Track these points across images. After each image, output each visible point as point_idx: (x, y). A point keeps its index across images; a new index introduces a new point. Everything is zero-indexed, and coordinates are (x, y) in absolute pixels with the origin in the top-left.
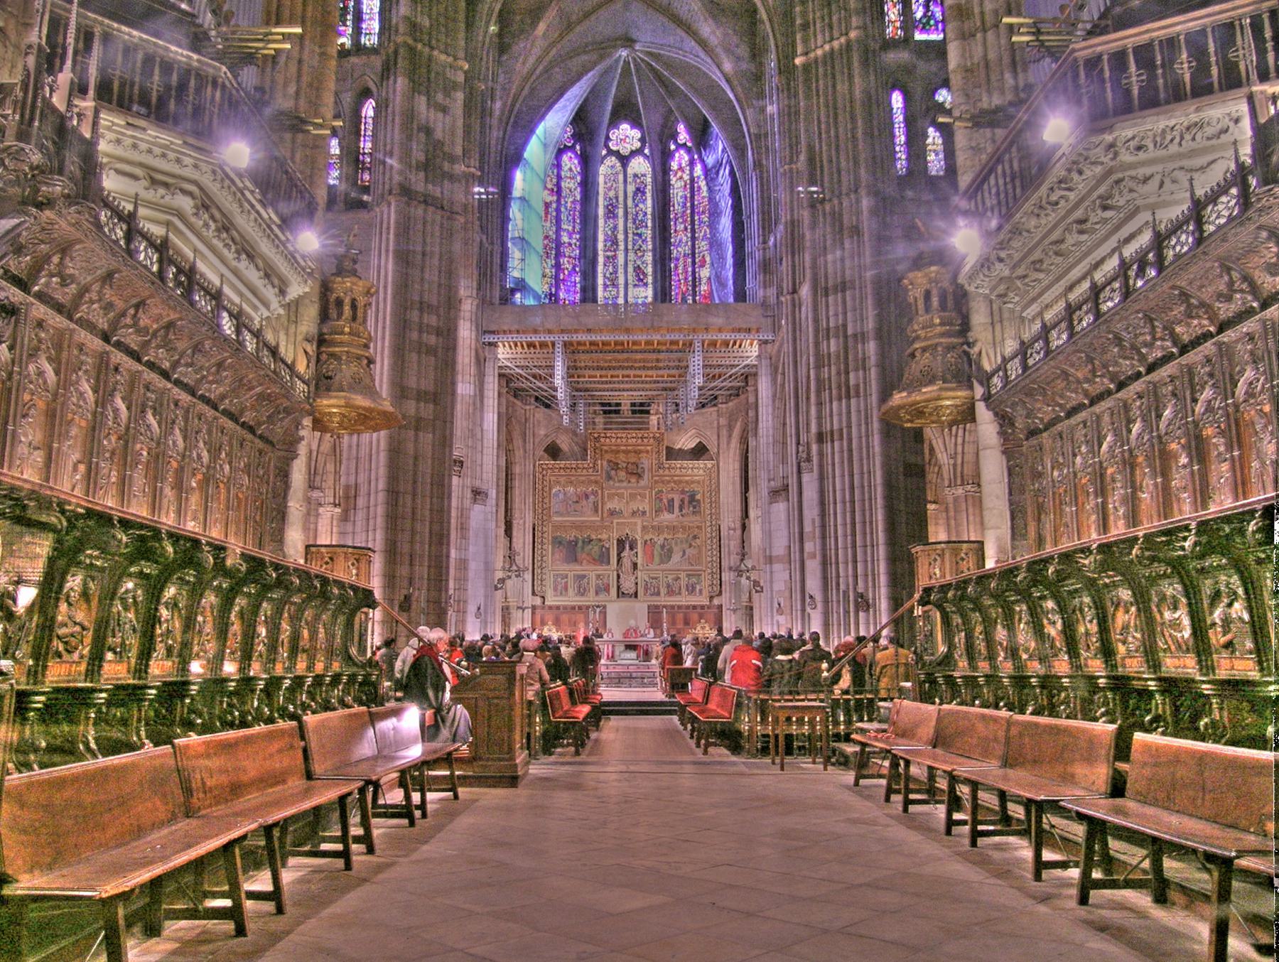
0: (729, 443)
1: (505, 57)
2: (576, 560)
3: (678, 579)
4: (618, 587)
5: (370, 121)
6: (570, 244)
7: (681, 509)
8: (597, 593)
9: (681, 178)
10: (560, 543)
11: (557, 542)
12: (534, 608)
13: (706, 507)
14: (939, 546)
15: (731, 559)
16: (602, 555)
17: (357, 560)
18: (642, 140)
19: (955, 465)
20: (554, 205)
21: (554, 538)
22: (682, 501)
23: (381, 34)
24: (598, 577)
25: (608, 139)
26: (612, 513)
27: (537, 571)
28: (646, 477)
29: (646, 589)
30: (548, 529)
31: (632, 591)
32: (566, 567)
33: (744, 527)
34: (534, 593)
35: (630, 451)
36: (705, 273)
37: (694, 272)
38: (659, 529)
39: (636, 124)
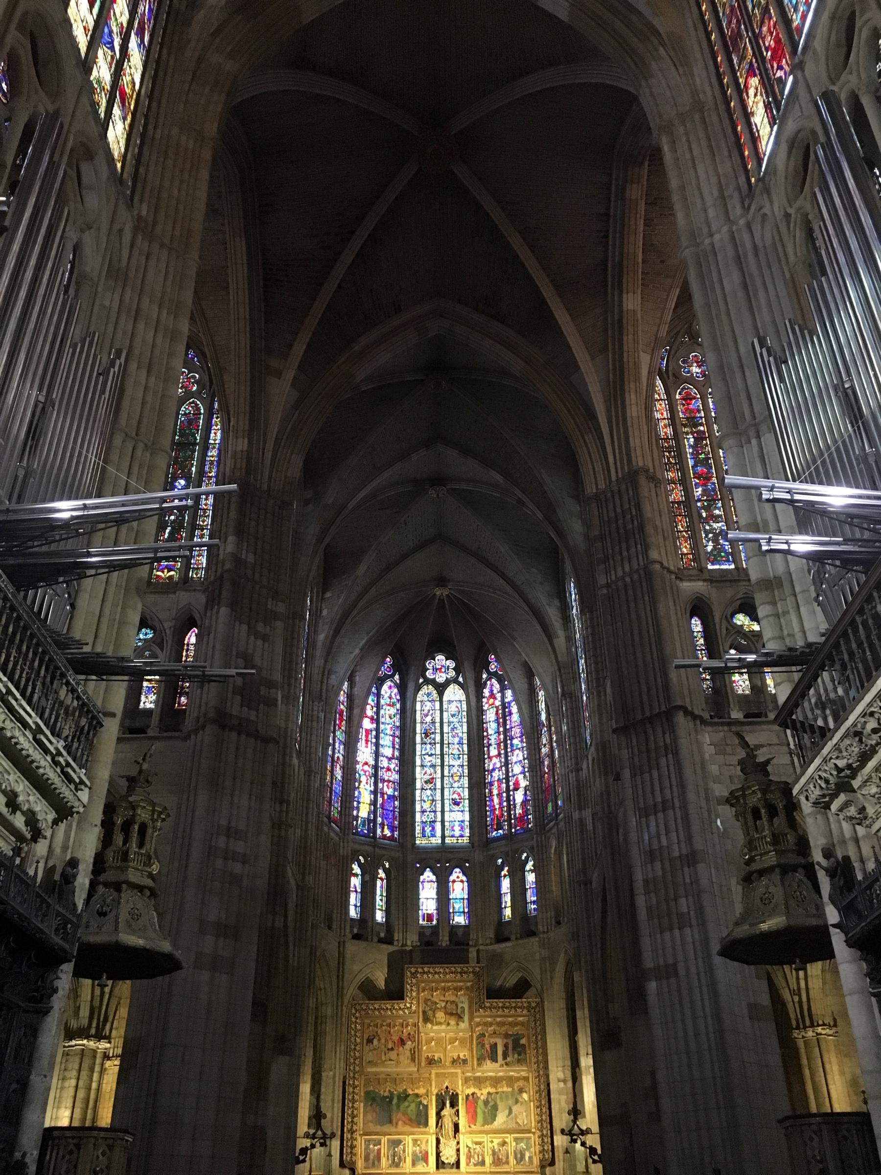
0: (552, 978)
1: (328, 595)
2: (391, 1122)
3: (504, 1143)
5: (192, 648)
6: (388, 769)
8: (414, 1164)
9: (493, 704)
10: (373, 1099)
11: (371, 1098)
13: (531, 1053)
14: (812, 1120)
15: (561, 1120)
17: (111, 1147)
18: (456, 669)
19: (800, 1002)
20: (374, 733)
21: (367, 1093)
22: (506, 1046)
23: (207, 569)
24: (415, 1141)
26: (431, 1062)
28: (466, 1018)
29: (469, 1157)
31: (453, 1160)
32: (378, 1129)
37: (508, 796)
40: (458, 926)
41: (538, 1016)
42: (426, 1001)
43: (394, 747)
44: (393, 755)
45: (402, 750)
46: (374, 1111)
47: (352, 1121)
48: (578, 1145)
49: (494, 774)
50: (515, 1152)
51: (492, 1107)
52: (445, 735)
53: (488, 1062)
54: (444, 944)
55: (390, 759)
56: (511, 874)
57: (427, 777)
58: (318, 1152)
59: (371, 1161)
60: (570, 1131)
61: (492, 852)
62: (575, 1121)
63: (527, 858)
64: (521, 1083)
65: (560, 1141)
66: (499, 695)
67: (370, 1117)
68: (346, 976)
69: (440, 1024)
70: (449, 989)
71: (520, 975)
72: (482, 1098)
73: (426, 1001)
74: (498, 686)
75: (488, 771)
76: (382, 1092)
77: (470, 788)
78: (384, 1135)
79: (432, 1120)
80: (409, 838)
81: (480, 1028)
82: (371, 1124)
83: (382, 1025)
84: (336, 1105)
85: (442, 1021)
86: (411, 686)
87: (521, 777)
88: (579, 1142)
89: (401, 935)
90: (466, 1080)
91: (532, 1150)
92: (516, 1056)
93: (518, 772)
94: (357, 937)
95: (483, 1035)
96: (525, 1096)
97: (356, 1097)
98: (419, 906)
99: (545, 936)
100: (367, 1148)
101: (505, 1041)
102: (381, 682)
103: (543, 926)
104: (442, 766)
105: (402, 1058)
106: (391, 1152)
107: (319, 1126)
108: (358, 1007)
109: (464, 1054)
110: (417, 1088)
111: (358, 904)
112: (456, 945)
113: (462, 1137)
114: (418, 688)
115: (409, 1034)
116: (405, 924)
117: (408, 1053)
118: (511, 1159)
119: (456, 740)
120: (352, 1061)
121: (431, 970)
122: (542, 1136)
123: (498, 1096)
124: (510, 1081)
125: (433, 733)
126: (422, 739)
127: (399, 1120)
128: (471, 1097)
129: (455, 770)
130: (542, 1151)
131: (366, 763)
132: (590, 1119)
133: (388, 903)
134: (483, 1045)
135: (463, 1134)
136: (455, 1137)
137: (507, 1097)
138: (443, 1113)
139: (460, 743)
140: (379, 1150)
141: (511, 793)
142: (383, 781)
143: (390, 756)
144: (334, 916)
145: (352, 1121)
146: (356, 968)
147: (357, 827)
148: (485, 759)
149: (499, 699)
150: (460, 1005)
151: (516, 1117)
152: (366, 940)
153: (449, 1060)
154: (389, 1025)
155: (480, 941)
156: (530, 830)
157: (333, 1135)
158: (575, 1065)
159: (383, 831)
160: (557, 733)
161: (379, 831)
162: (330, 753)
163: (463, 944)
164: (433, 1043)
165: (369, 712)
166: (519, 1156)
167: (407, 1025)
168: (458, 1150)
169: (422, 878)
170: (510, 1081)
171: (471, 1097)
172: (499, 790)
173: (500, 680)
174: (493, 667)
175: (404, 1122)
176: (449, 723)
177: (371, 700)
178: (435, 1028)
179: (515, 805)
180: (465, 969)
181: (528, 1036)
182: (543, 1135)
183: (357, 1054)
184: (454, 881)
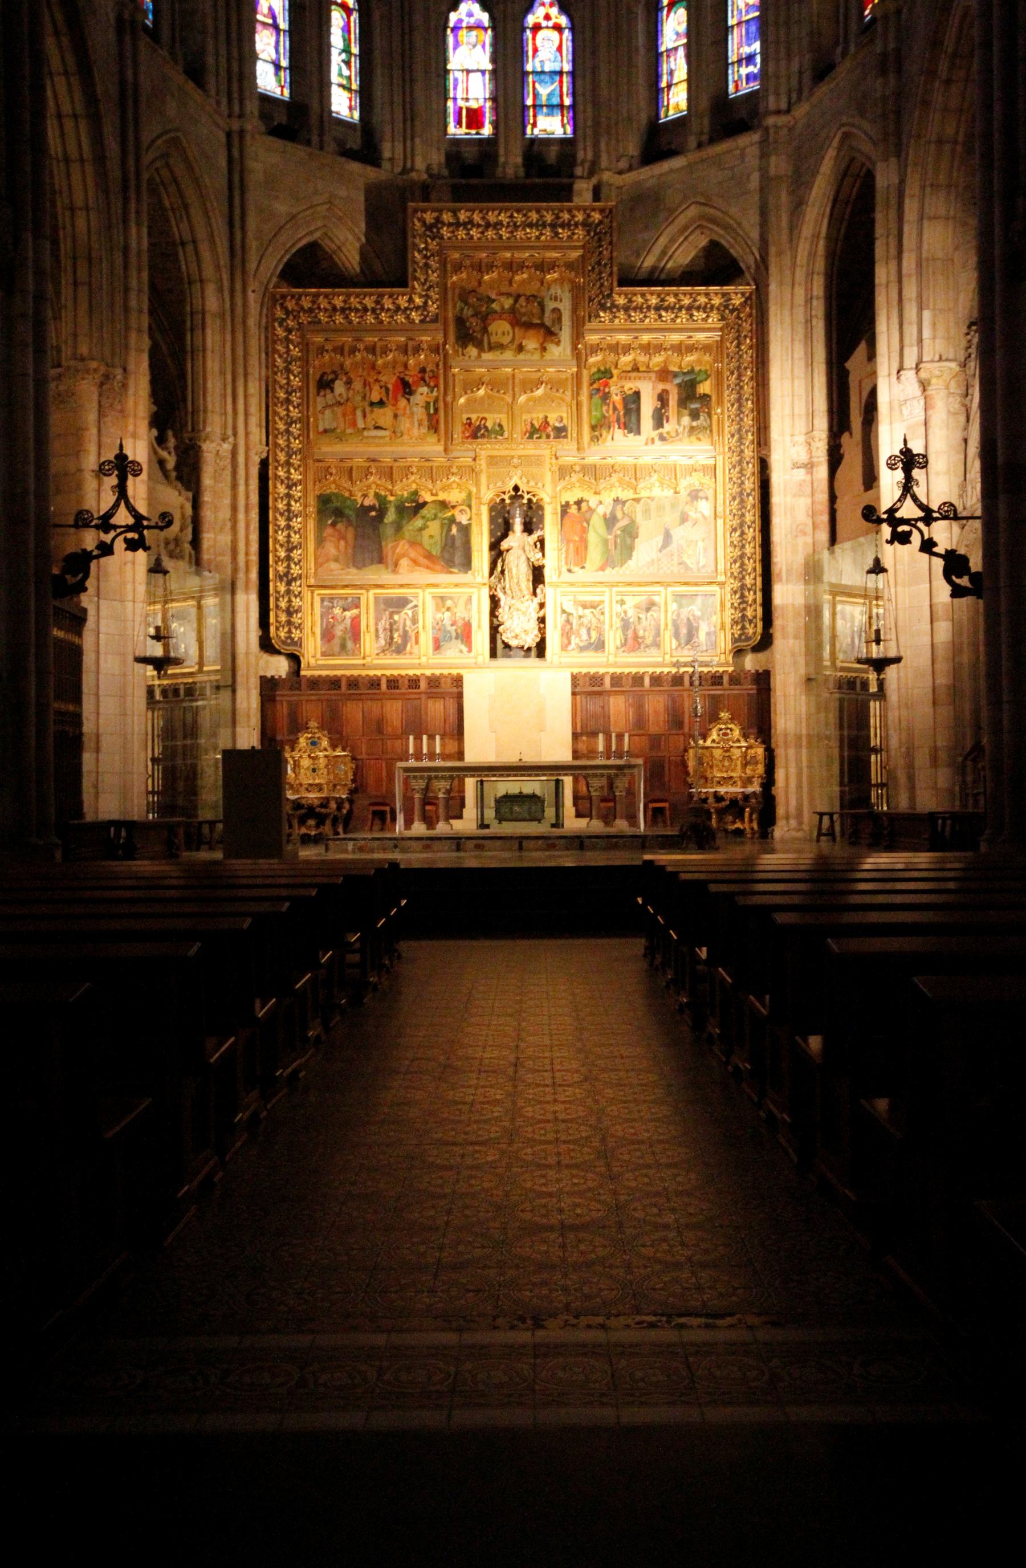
0: (794, 228)
2: (381, 560)
4: (494, 630)
7: (659, 419)
8: (437, 646)
12: (269, 686)
13: (723, 412)
16: (449, 544)
22: (663, 399)
27: (277, 587)
28: (566, 334)
29: (567, 634)
31: (530, 640)
32: (353, 575)
34: (267, 645)
35: (522, 266)
38: (594, 473)
40: (548, 142)
46: (343, 537)
47: (289, 558)
50: (674, 621)
51: (624, 530)
53: (618, 433)
54: (510, 171)
59: (336, 641)
60: (891, 511)
64: (695, 480)
67: (330, 548)
68: (252, 223)
69: (501, 347)
70: (522, 266)
71: (703, 242)
72: (601, 510)
73: (464, 295)
76: (360, 501)
79: (481, 556)
81: (599, 358)
82: (333, 565)
83: (353, 350)
84: (241, 516)
85: (506, 340)
89: (399, 148)
90: (564, 472)
92: (686, 420)
96: (705, 507)
97: (296, 507)
98: (446, 90)
99: (782, 120)
100: (326, 613)
101: (661, 386)
103: (777, 94)
105: (405, 424)
106: (384, 623)
108: (290, 305)
110: (444, 489)
111: (284, 63)
112: (539, 176)
113: (548, 591)
115: (423, 370)
116: (410, 116)
117: (420, 412)
120: (281, 426)
121: (477, 218)
122: (741, 591)
123: (639, 508)
127: (404, 555)
128: (573, 509)
130: (742, 621)
133: (366, 73)
134: (606, 397)
136: (535, 594)
137: (660, 508)
138: (504, 545)
140: (356, 622)
144: (210, 60)
145: (289, 558)
146: (282, 208)
150: (550, 305)
152: (308, 143)
153: (521, 428)
154: (372, 349)
155: (604, 162)
163: (558, 174)
164: (482, 392)
166: (684, 631)
167: (417, 350)
168: (542, 620)
169: (453, 17)
170: (673, 472)
171: (573, 509)
175: (415, 562)
178: (487, 356)
180: (566, 216)
181: (719, 373)
182: (743, 587)
184: (537, 28)
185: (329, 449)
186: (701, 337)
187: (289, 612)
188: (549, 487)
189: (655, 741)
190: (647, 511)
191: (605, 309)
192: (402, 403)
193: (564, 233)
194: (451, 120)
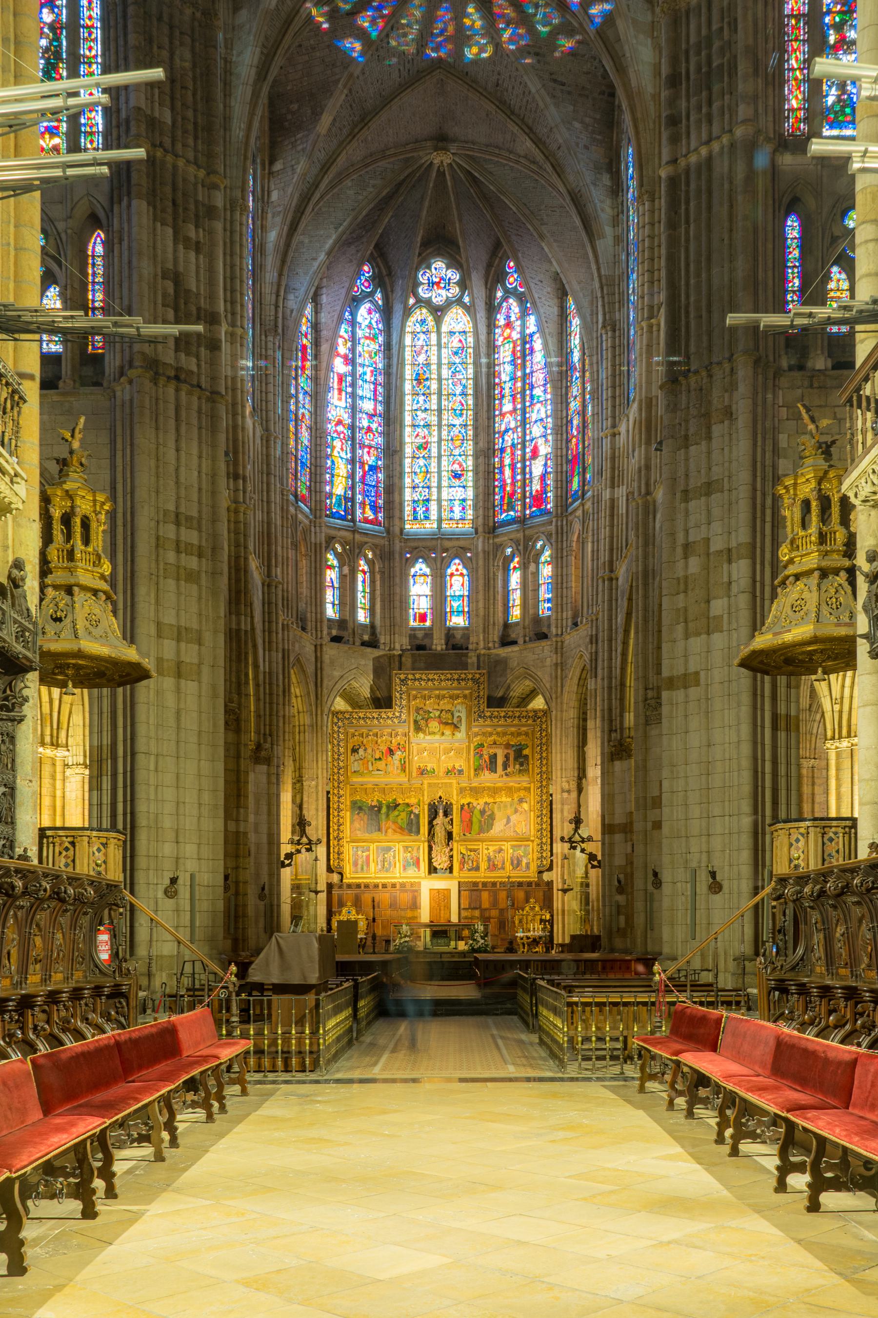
2: (379, 830)
6: (369, 429)
7: (505, 768)
8: (405, 868)
9: (509, 337)
10: (360, 808)
11: (357, 807)
13: (534, 765)
15: (562, 828)
16: (410, 823)
18: (463, 284)
20: (349, 379)
21: (354, 803)
22: (507, 757)
25: (416, 284)
26: (422, 772)
28: (463, 727)
29: (463, 863)
30: (345, 792)
31: (446, 865)
33: (580, 790)
36: (537, 468)
37: (524, 467)
38: (476, 791)
39: (454, 262)
41: (544, 726)
42: (418, 710)
43: (375, 399)
44: (375, 410)
45: (387, 403)
48: (578, 852)
49: (506, 438)
52: (444, 382)
53: (487, 772)
55: (371, 416)
56: (524, 566)
57: (420, 440)
58: (303, 857)
59: (359, 866)
61: (497, 540)
62: (576, 830)
63: (543, 547)
65: (560, 848)
66: (519, 323)
69: (434, 733)
70: (444, 697)
72: (478, 807)
73: (418, 710)
74: (517, 310)
75: (499, 432)
77: (476, 456)
78: (373, 842)
80: (397, 521)
83: (367, 736)
86: (398, 309)
87: (541, 441)
88: (579, 849)
91: (530, 856)
92: (517, 767)
93: (538, 435)
94: (336, 639)
95: (482, 745)
96: (525, 806)
97: (342, 806)
100: (356, 854)
101: (506, 751)
102: (355, 302)
104: (440, 426)
105: (390, 768)
106: (380, 858)
107: (303, 833)
108: (340, 716)
109: (460, 764)
114: (407, 312)
117: (397, 763)
118: (508, 865)
119: (458, 390)
123: (496, 806)
124: (510, 791)
125: (427, 379)
126: (413, 387)
129: (455, 431)
131: (339, 422)
132: (592, 826)
134: (481, 756)
135: (457, 841)
137: (505, 806)
139: (464, 394)
140: (368, 857)
141: (528, 463)
142: (365, 446)
143: (372, 412)
146: (337, 674)
147: (331, 509)
148: (495, 416)
149: (518, 329)
150: (456, 714)
151: (515, 826)
154: (376, 735)
156: (548, 512)
157: (319, 841)
158: (582, 775)
159: (364, 512)
160: (592, 381)
161: (358, 512)
162: (293, 408)
165: (342, 350)
167: (397, 735)
172: (512, 460)
173: (521, 299)
174: (512, 280)
176: (451, 364)
177: (344, 330)
178: (428, 737)
179: (531, 478)
180: (463, 676)
183: (341, 764)
185: (356, 779)
186: (524, 729)
187: (339, 854)
188: (455, 797)
189: (502, 911)
190: (499, 808)
191: (480, 717)
192: (390, 758)
193: (463, 683)
194: (411, 618)
